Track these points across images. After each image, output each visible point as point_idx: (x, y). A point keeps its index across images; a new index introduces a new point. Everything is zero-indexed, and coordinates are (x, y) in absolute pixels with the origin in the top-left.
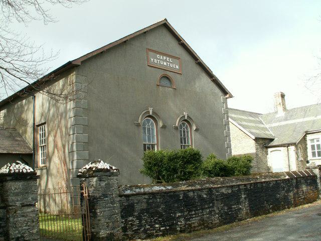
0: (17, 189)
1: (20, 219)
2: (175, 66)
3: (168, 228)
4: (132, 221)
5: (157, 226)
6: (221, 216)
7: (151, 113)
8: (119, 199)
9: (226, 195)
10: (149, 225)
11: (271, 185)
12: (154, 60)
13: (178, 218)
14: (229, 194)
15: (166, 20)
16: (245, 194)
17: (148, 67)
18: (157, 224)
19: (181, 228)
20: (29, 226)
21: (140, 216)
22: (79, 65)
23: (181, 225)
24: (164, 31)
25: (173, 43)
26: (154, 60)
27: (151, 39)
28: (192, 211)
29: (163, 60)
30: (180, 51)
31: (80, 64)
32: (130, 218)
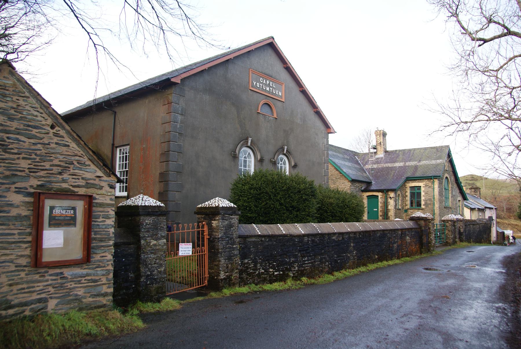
0: (148, 224)
1: (149, 256)
2: (278, 93)
3: (281, 273)
4: (248, 263)
5: (271, 270)
6: (331, 264)
7: (285, 152)
8: (238, 240)
9: (336, 242)
10: (263, 269)
11: (378, 235)
12: (256, 84)
13: (292, 263)
14: (339, 240)
15: (273, 38)
16: (354, 243)
17: (250, 91)
18: (271, 268)
19: (294, 274)
20: (157, 264)
21: (255, 259)
22: (178, 83)
23: (294, 271)
24: (270, 52)
25: (279, 66)
26: (256, 84)
27: (255, 61)
28: (304, 257)
29: (266, 84)
30: (284, 75)
31: (179, 82)
32: (246, 261)
